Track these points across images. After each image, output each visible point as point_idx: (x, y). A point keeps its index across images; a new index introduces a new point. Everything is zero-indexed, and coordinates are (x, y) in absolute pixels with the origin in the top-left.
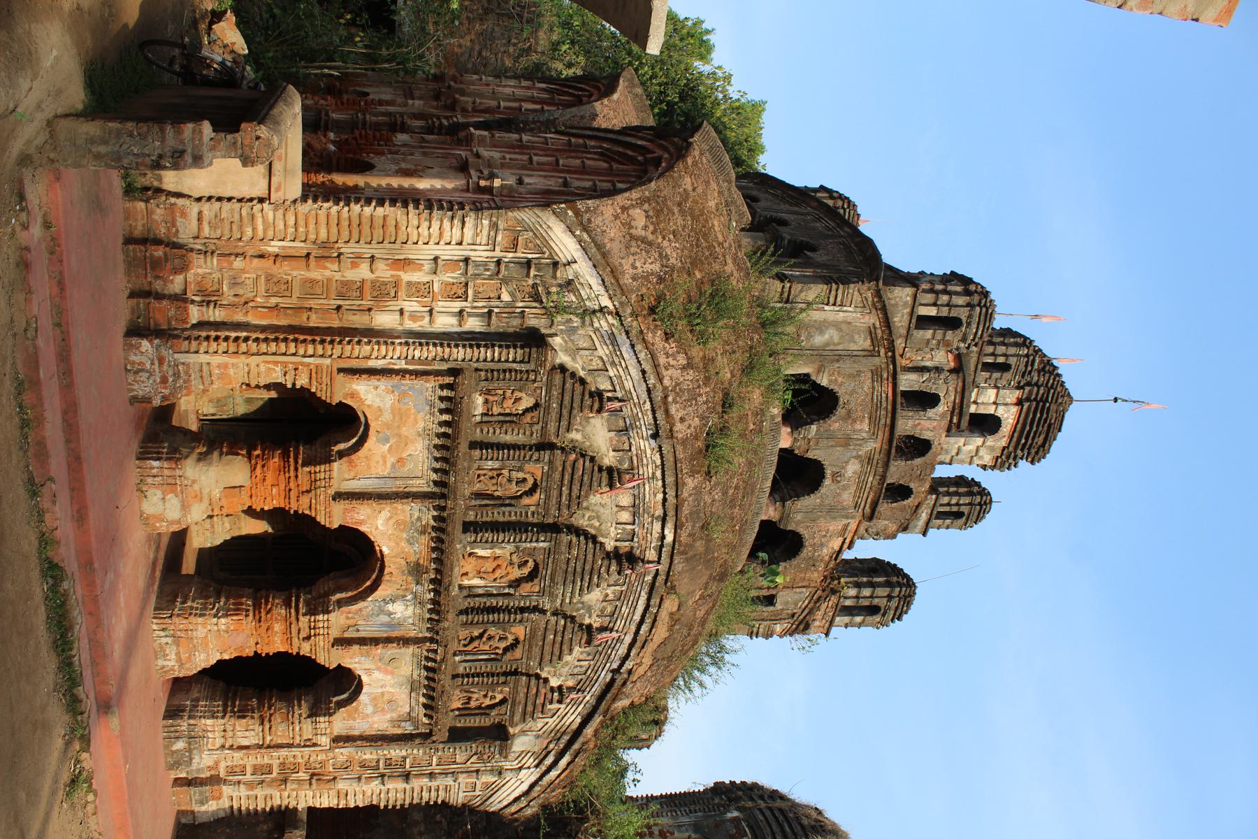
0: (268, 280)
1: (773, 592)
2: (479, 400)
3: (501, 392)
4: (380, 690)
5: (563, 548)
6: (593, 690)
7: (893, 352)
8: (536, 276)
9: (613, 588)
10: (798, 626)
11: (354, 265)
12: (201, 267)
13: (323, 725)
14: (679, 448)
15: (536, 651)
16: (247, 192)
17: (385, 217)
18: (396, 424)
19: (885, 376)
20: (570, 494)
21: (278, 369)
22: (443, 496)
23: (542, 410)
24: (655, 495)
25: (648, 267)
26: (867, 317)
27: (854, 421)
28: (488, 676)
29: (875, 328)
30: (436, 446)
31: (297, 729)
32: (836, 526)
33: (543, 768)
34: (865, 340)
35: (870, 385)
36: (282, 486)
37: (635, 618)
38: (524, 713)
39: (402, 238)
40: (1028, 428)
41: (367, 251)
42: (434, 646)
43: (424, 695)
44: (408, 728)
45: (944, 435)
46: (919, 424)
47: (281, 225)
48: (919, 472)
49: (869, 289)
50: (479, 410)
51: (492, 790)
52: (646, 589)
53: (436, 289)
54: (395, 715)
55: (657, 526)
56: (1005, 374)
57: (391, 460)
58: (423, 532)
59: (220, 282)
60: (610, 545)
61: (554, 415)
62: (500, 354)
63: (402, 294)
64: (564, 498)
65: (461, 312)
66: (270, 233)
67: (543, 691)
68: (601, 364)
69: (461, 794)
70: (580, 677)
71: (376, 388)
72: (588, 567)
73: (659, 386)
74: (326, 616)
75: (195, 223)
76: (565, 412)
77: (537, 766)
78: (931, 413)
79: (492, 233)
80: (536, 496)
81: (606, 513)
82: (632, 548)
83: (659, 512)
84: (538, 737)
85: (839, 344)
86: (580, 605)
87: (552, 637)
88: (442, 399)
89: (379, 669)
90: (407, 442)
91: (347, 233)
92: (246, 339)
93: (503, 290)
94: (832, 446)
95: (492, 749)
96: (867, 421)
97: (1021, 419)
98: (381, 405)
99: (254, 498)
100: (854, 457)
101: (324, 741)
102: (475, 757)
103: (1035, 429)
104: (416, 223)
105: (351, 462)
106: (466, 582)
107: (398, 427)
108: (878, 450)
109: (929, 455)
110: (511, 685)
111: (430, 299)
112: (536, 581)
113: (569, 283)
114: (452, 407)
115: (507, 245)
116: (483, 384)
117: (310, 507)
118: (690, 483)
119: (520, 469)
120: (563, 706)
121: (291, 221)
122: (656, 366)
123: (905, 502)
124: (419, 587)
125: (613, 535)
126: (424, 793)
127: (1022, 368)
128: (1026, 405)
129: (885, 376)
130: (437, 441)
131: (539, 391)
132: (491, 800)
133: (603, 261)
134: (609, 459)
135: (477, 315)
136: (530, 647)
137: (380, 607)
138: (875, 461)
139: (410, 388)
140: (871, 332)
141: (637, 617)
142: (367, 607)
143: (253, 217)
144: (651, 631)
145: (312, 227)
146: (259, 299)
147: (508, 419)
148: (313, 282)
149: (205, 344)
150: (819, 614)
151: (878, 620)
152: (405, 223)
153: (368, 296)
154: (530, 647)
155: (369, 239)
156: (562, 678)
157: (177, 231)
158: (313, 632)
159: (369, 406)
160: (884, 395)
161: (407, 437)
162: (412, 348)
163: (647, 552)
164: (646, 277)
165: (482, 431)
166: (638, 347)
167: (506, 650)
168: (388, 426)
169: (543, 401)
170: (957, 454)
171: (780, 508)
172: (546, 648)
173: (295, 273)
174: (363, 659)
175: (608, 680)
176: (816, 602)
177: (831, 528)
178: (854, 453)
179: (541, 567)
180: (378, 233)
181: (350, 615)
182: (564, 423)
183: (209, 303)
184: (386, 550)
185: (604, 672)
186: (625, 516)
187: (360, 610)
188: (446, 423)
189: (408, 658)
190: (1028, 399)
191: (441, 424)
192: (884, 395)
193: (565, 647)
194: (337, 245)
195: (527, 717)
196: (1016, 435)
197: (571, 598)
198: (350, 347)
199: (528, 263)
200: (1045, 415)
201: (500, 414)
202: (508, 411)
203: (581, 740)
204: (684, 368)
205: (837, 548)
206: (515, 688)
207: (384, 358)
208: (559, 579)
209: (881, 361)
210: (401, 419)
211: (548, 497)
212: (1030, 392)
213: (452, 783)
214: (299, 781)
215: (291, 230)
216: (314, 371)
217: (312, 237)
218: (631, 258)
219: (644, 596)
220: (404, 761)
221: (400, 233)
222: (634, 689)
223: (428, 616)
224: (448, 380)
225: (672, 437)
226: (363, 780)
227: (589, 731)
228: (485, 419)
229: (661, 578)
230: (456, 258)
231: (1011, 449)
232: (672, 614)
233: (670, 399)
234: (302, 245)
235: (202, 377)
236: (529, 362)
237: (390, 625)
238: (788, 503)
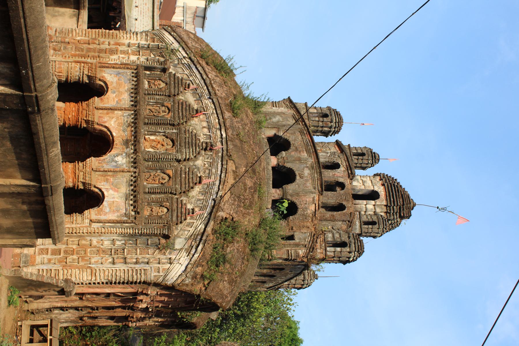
1: (291, 234)
2: (147, 83)
4: (112, 200)
5: (183, 132)
6: (207, 210)
7: (304, 121)
8: (161, 48)
9: (206, 160)
10: (309, 250)
11: (103, 43)
12: (55, 42)
13: (86, 215)
14: (219, 99)
15: (178, 180)
16: (70, 27)
17: (113, 33)
19: (305, 132)
20: (182, 114)
22: (136, 106)
24: (215, 120)
25: (196, 45)
26: (290, 111)
27: (300, 152)
28: (159, 198)
29: (294, 115)
30: (132, 93)
31: (75, 218)
32: (309, 198)
33: (191, 256)
34: (292, 120)
35: (301, 137)
36: (77, 107)
37: (218, 173)
38: (177, 216)
40: (391, 193)
41: (108, 40)
42: (135, 170)
43: (131, 200)
44: (125, 219)
45: (348, 180)
46: (335, 174)
47: (81, 34)
48: (344, 197)
49: (287, 101)
50: (146, 86)
51: (168, 271)
52: (220, 159)
53: (130, 52)
54: (119, 214)
55: (219, 132)
56: (364, 157)
57: (116, 100)
58: (128, 126)
59: (60, 48)
60: (202, 140)
61: (173, 86)
63: (119, 53)
64: (180, 115)
67: (184, 206)
68: (187, 77)
69: (152, 275)
70: (200, 206)
71: (111, 75)
72: (194, 142)
73: (207, 78)
74: (90, 158)
75: (54, 32)
76: (176, 85)
77: (187, 256)
78: (338, 170)
80: (170, 114)
81: (198, 127)
82: (211, 143)
83: (218, 127)
84: (186, 239)
85: (283, 122)
86: (194, 167)
87: (184, 176)
88: (133, 76)
89: (112, 189)
90: (121, 93)
94: (294, 160)
95: (164, 231)
96: (305, 152)
97: (387, 190)
98: (113, 81)
99: (66, 112)
100: (306, 167)
101: (87, 221)
102: (157, 250)
103: (394, 194)
104: (122, 34)
105: (102, 99)
106: (146, 150)
107: (119, 88)
108: (314, 162)
109: (345, 189)
110: (170, 202)
112: (174, 147)
113: (172, 50)
114: (137, 75)
117: (86, 117)
118: (227, 115)
119: (163, 105)
120: (195, 221)
121: (84, 32)
122: (205, 71)
123: (344, 211)
124: (128, 149)
125: (202, 137)
126: (134, 274)
127: (370, 153)
128: (386, 185)
129: (305, 132)
130: (132, 91)
132: (168, 277)
133: (182, 41)
134: (196, 107)
136: (176, 179)
137: (112, 159)
138: (315, 168)
140: (294, 117)
141: (219, 172)
142: (107, 158)
144: (226, 175)
150: (318, 245)
151: (348, 250)
153: (107, 52)
154: (176, 179)
156: (192, 205)
158: (84, 167)
160: (308, 140)
163: (217, 144)
164: (197, 47)
166: (198, 66)
167: (165, 183)
168: (115, 88)
170: (366, 210)
171: (282, 190)
172: (183, 180)
173: (84, 46)
174: (105, 183)
175: (213, 204)
176: (314, 236)
177: (307, 200)
178: (305, 165)
179: (175, 141)
180: (111, 37)
181: (100, 162)
182: (176, 89)
184: (114, 134)
185: (210, 201)
186: (206, 131)
187: (104, 159)
188: (135, 82)
189: (124, 184)
190: (386, 182)
192: (308, 140)
193: (190, 180)
195: (179, 218)
196: (388, 198)
197: (189, 154)
199: (159, 45)
200: (396, 189)
203: (206, 234)
204: (215, 76)
205: (314, 210)
206: (172, 203)
208: (183, 144)
209: (301, 126)
210: (119, 85)
211: (174, 114)
212: (386, 180)
213: (147, 267)
214: (73, 259)
215: (84, 35)
217: (91, 37)
218: (191, 41)
219: (219, 161)
220: (124, 252)
222: (225, 207)
223: (132, 160)
224: (135, 67)
225: (216, 95)
226: (104, 259)
227: (209, 229)
229: (225, 152)
231: (389, 205)
232: (233, 171)
233: (212, 82)
237: (116, 166)
238: (284, 186)
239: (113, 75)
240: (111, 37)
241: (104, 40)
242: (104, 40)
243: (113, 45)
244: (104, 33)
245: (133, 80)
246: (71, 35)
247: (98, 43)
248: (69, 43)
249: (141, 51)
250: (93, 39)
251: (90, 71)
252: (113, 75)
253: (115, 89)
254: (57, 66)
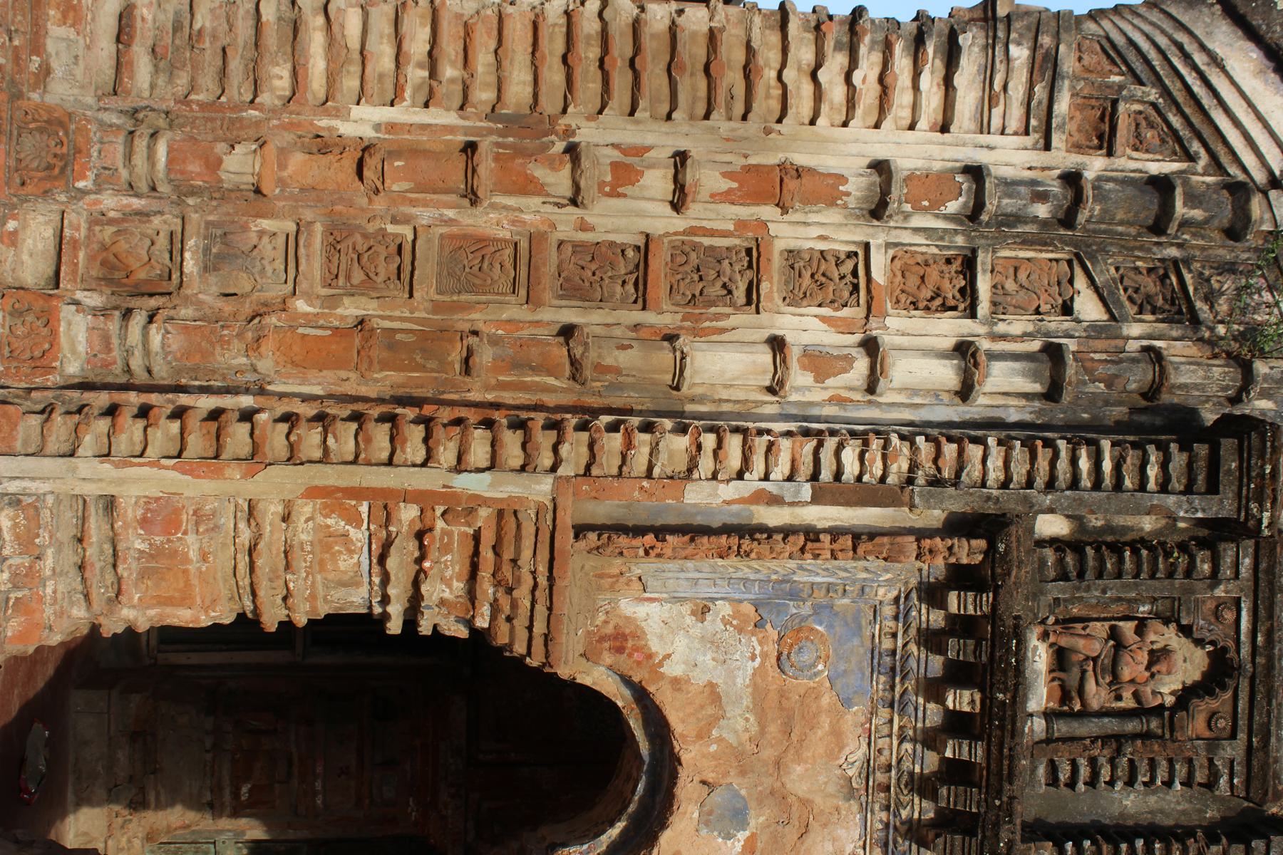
0: (333, 247)
2: (1039, 657)
3: (1100, 629)
17: (713, 37)
18: (768, 753)
21: (358, 535)
23: (1244, 685)
39: (766, 102)
47: (387, 63)
53: (878, 275)
62: (1117, 468)
63: (770, 288)
65: (964, 350)
66: (351, 83)
71: (702, 612)
75: (106, 47)
79: (1040, 91)
88: (931, 640)
91: (595, 86)
92: (247, 416)
93: (1081, 282)
107: (778, 764)
111: (860, 312)
115: (1077, 137)
116: (1056, 590)
121: (418, 45)
131: (1229, 616)
135: (1015, 357)
139: (817, 610)
143: (295, 28)
145: (483, 59)
146: (301, 305)
147: (1131, 726)
148: (481, 245)
149: (103, 425)
152: (774, 57)
155: (665, 108)
157: (46, 71)
159: (676, 683)
161: (805, 802)
162: (831, 443)
165: (1053, 768)
168: (741, 760)
169: (1245, 651)
173: (424, 215)
180: (692, 86)
183: (127, 314)
191: (930, 740)
194: (563, 122)
198: (617, 439)
201: (1104, 713)
202: (1128, 702)
207: (740, 476)
215: (416, 74)
216: (488, 539)
217: (483, 95)
221: (760, 90)
224: (969, 552)
228: (1062, 728)
230: (937, 166)
234: (451, 118)
235: (81, 567)
236: (1213, 488)
239: (724, 609)
240: (692, 86)
241: (630, 134)
242: (630, 134)
243: (727, 197)
244: (621, 47)
245: (934, 690)
246: (279, 78)
247: (565, 189)
248: (258, 191)
249: (983, 259)
250: (514, 123)
251: (487, 589)
252: (724, 609)
253: (743, 773)
254: (136, 542)
